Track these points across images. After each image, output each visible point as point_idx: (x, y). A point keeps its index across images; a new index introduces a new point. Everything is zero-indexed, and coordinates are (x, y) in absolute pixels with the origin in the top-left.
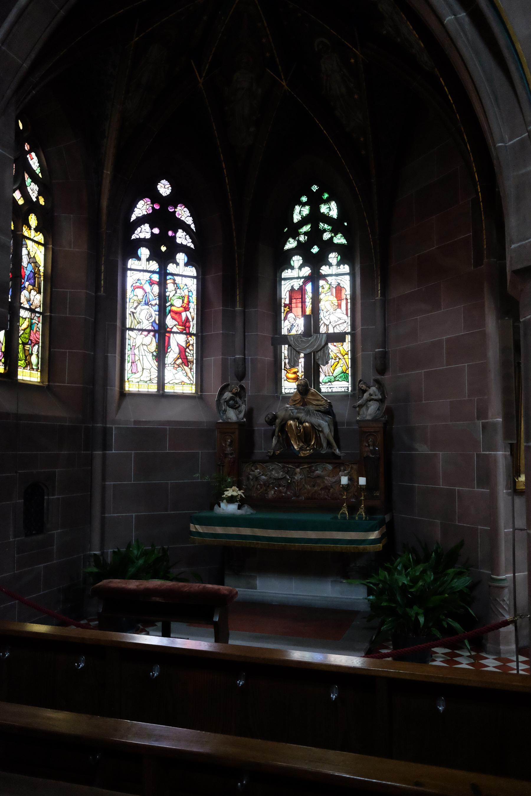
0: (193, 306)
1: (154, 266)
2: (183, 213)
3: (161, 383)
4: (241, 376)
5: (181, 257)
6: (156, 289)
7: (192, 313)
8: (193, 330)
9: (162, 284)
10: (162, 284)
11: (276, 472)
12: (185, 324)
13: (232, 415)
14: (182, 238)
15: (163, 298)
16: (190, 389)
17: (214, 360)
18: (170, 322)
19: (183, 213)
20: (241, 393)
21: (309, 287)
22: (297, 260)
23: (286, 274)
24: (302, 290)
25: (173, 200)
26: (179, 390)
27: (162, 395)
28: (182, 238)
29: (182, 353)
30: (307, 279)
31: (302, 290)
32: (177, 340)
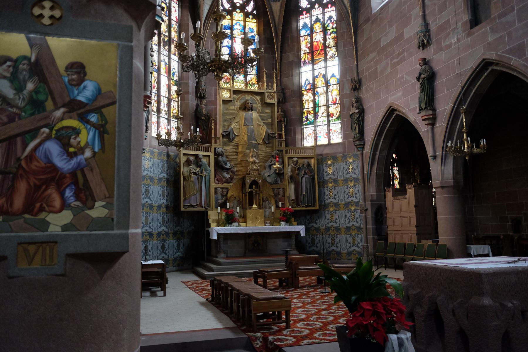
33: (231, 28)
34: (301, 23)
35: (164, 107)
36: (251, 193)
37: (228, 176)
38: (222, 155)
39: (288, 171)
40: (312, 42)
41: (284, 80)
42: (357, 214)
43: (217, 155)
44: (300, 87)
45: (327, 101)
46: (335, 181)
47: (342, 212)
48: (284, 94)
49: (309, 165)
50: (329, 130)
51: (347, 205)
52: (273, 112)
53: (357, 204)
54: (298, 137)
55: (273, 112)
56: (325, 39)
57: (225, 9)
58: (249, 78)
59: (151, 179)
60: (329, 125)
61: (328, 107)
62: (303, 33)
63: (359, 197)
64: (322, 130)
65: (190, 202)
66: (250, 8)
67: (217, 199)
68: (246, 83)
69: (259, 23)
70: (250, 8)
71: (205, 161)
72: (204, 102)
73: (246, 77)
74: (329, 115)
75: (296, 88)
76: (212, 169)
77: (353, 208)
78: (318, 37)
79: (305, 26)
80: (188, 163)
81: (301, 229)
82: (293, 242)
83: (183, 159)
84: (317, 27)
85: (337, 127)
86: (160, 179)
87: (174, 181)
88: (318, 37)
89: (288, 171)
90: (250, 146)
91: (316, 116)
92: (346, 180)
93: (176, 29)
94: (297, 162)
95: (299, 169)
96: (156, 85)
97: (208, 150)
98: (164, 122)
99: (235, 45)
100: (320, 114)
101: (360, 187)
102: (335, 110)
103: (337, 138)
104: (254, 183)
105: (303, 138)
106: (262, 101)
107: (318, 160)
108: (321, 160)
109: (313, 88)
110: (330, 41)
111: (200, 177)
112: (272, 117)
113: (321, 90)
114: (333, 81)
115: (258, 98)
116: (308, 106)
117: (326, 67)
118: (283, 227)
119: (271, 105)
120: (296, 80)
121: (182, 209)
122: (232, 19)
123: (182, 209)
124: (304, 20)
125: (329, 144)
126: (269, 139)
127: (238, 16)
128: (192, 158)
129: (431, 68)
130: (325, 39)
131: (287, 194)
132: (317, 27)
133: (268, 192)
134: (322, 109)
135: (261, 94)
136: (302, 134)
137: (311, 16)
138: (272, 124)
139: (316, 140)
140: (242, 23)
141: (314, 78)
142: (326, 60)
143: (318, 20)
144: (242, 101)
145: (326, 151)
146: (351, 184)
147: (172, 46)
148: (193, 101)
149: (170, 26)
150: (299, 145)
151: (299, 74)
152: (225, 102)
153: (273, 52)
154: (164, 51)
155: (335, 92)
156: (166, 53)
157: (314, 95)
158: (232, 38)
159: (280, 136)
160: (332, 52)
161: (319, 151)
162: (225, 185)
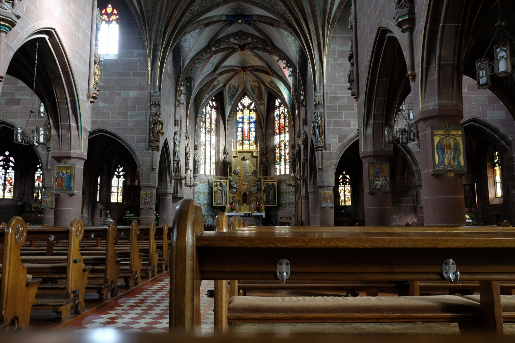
0: (13, 179)
1: (4, 171)
2: (12, 159)
3: (4, 196)
4: (24, 195)
5: (11, 168)
6: (4, 176)
7: (13, 181)
8: (13, 184)
9: (5, 175)
10: (5, 175)
11: (28, 215)
12: (11, 184)
13: (19, 203)
14: (11, 164)
15: (5, 178)
16: (11, 198)
17: (17, 191)
18: (7, 183)
19: (12, 159)
20: (22, 199)
21: (42, 176)
22: (39, 170)
23: (37, 172)
24: (40, 177)
25: (9, 156)
26: (8, 198)
27: (4, 199)
28: (11, 164)
29: (10, 190)
30: (41, 174)
31: (40, 177)
32: (8, 187)
33: (243, 118)
34: (276, 114)
35: (208, 160)
36: (245, 198)
37: (234, 190)
38: (232, 181)
39: (263, 188)
40: (280, 123)
41: (267, 142)
42: (293, 208)
43: (230, 181)
44: (274, 146)
45: (285, 153)
46: (286, 192)
47: (288, 207)
48: (266, 149)
49: (273, 184)
50: (285, 168)
51: (290, 204)
52: (257, 160)
53: (293, 203)
54: (272, 171)
55: (257, 160)
56: (285, 122)
57: (240, 109)
58: (251, 142)
59: (200, 193)
60: (285, 165)
61: (285, 156)
62: (277, 118)
63: (294, 201)
64: (283, 167)
65: (218, 202)
66: (252, 107)
67: (230, 201)
68: (250, 145)
69: (256, 114)
70: (252, 107)
71: (224, 184)
72: (228, 156)
73: (249, 142)
74: (285, 160)
75: (271, 146)
76: (227, 188)
77: (292, 205)
78: (282, 121)
79: (277, 115)
80: (217, 185)
81: (263, 214)
82: (261, 220)
83: (214, 184)
84: (282, 116)
85: (288, 166)
86: (204, 193)
87: (211, 193)
88: (282, 121)
89: (263, 188)
90: (246, 176)
91: (280, 161)
92: (289, 192)
93: (215, 123)
94: (267, 184)
95: (268, 187)
96: (204, 151)
97: (227, 179)
98: (208, 168)
99: (244, 126)
100: (282, 160)
101: (294, 195)
102: (287, 158)
103: (288, 173)
104: (245, 194)
105: (275, 171)
106: (252, 155)
107: (278, 182)
108: (279, 182)
109: (280, 146)
110: (287, 123)
111: (222, 191)
112: (257, 163)
113: (283, 148)
114: (287, 144)
115: (250, 154)
116: (278, 155)
117: (285, 137)
118: (256, 213)
119: (256, 157)
120: (272, 143)
121: (214, 205)
122: (243, 114)
123: (214, 205)
124: (277, 112)
125: (285, 174)
126: (254, 173)
127: (246, 111)
128: (218, 183)
129: (300, 148)
130: (285, 122)
131: (262, 199)
132: (282, 116)
133: (253, 198)
134: (283, 157)
135: (252, 152)
136: (275, 169)
137: (279, 110)
138: (257, 166)
139: (280, 173)
140: (248, 115)
141: (280, 141)
142: (285, 133)
143: (282, 113)
144: (242, 156)
145: (283, 178)
146: (291, 194)
147: (212, 132)
148: (222, 156)
149: (211, 124)
150: (272, 175)
151: (274, 140)
152: (234, 157)
153: (262, 129)
154: (208, 136)
155: (287, 151)
156: (209, 136)
157: (280, 150)
158: (243, 123)
159: (261, 172)
160: (287, 129)
161: (279, 178)
162: (234, 195)
